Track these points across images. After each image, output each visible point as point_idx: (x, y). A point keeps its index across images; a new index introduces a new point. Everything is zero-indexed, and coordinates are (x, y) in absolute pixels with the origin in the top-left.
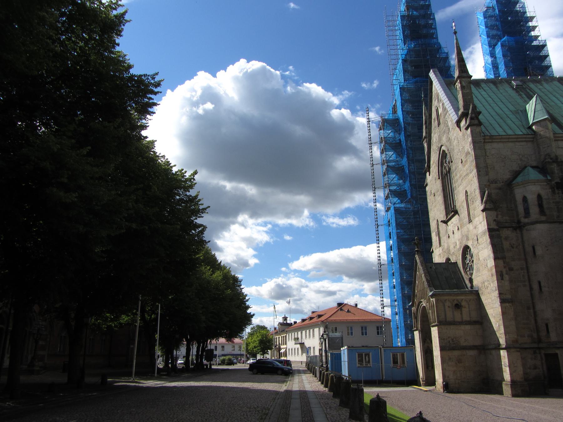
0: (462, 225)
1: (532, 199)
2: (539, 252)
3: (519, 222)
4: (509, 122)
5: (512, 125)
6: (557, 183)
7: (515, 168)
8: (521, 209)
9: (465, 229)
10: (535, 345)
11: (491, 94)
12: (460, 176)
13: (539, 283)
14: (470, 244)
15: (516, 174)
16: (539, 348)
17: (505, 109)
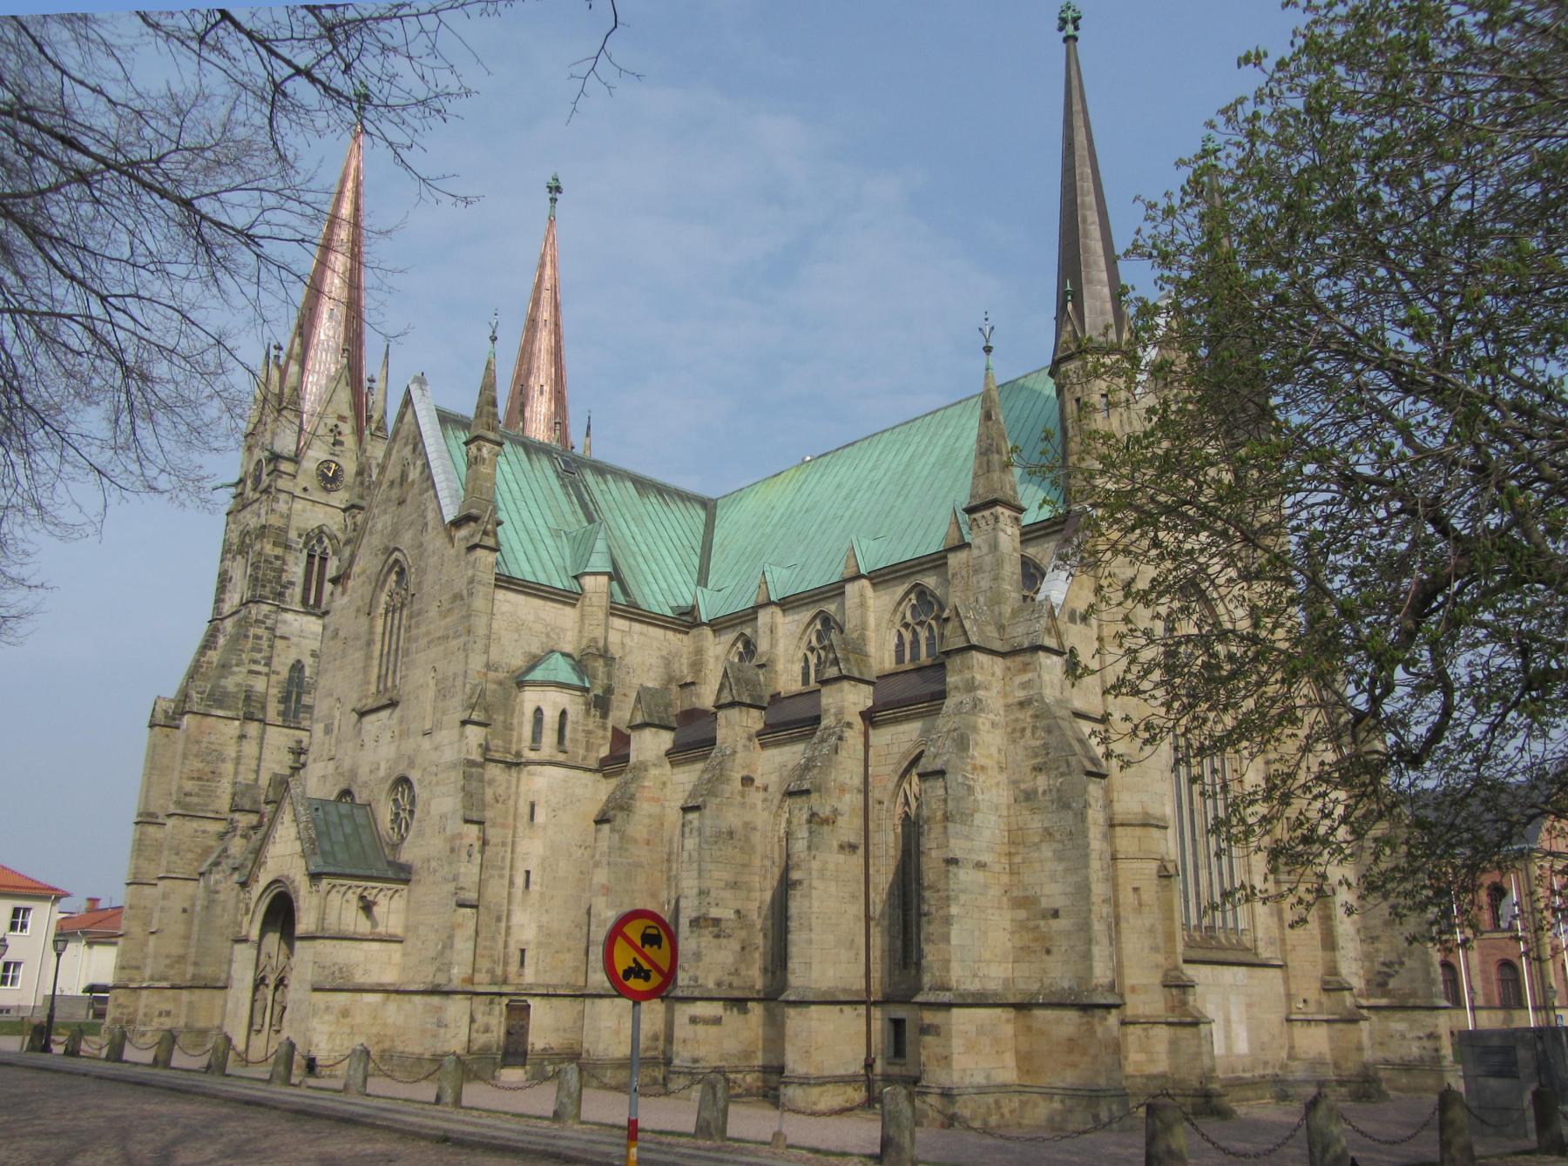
0: (404, 734)
1: (550, 718)
2: (540, 817)
3: (518, 754)
4: (544, 554)
5: (550, 565)
6: (596, 696)
7: (535, 648)
8: (527, 730)
9: (409, 745)
10: (495, 989)
11: (520, 476)
12: (428, 633)
13: (528, 873)
14: (414, 776)
15: (534, 662)
16: (501, 994)
17: (540, 521)
